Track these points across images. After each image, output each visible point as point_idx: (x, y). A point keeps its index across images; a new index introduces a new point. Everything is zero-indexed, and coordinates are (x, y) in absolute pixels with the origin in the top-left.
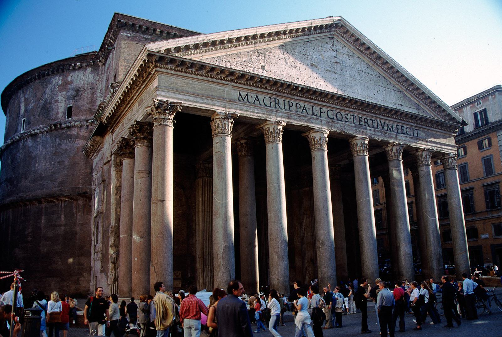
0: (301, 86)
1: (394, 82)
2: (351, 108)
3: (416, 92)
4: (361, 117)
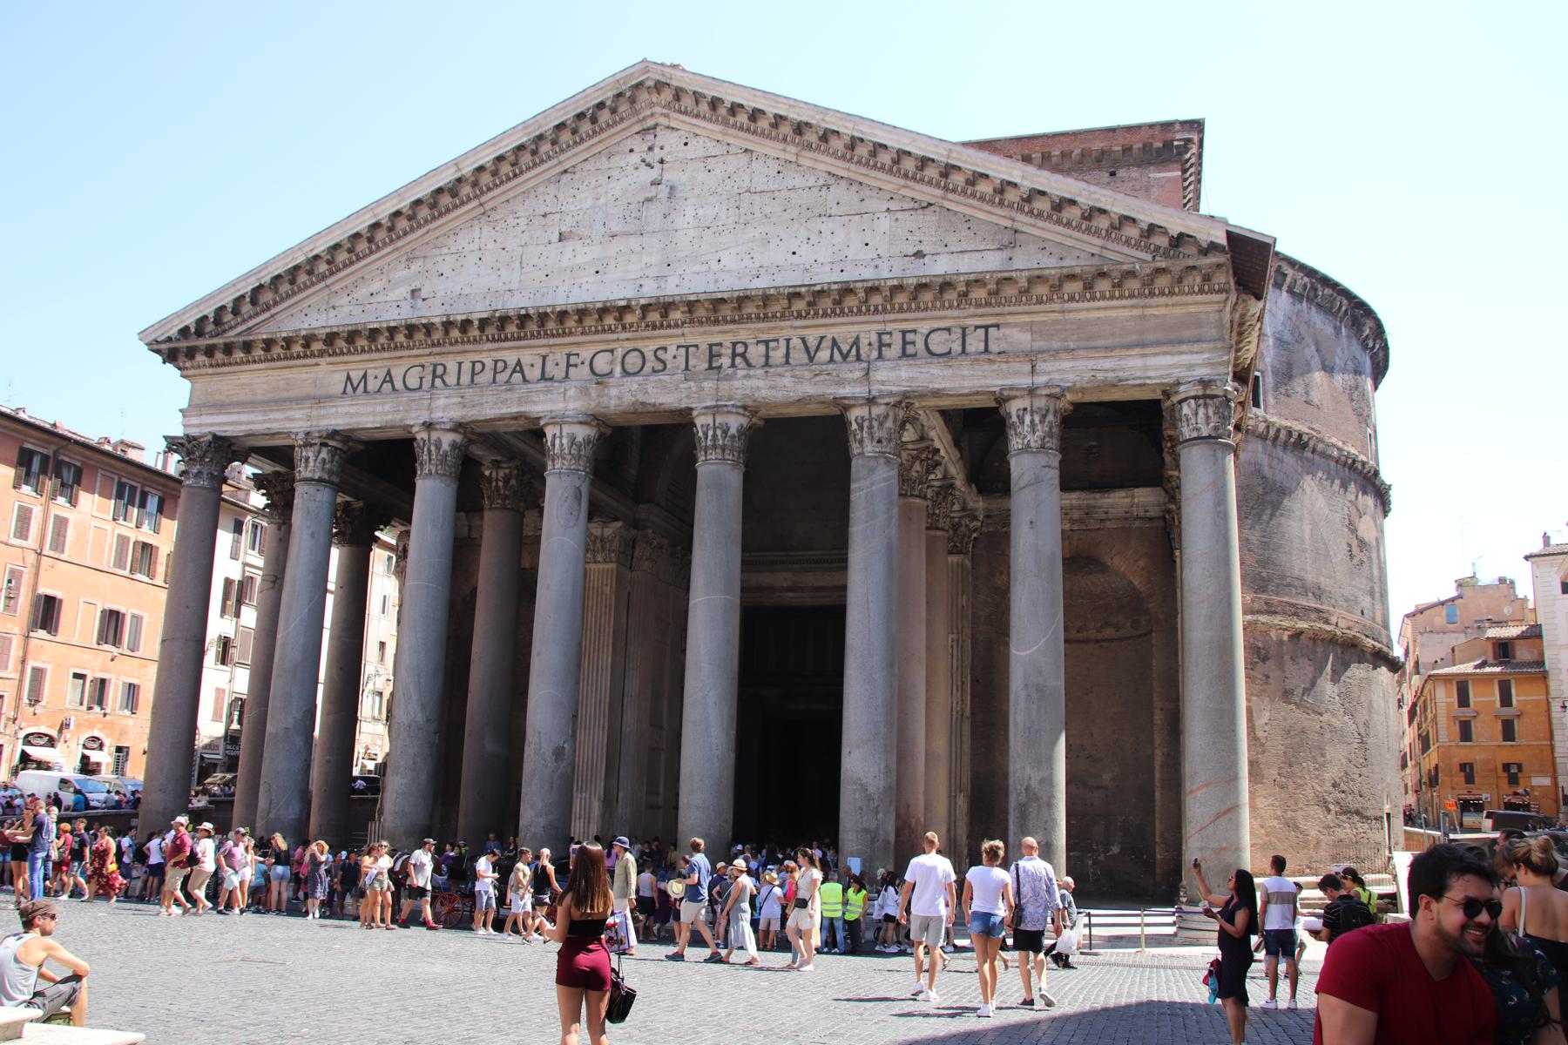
1: (891, 183)
2: (669, 326)
3: (984, 188)
4: (720, 344)
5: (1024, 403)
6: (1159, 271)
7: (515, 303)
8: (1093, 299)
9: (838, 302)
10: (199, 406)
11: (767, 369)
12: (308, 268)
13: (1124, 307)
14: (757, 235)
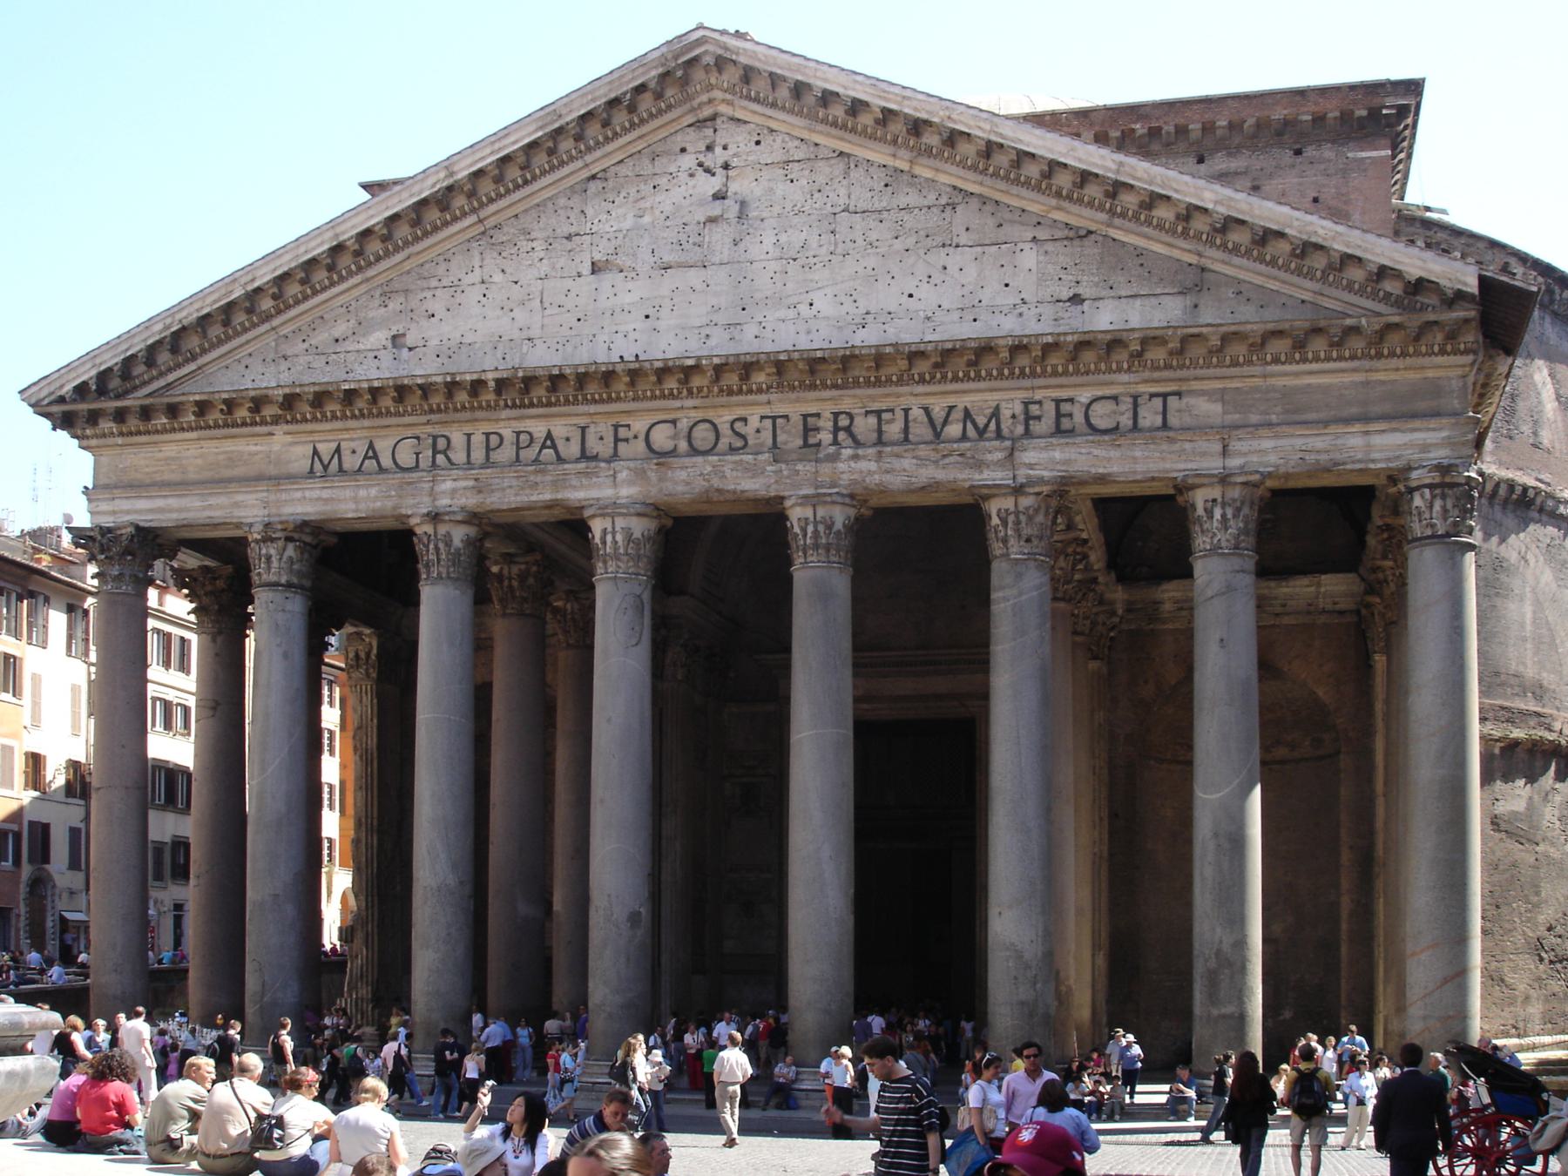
0: (490, 376)
2: (750, 391)
3: (1163, 213)
4: (818, 415)
6: (1390, 327)
7: (542, 358)
8: (1304, 360)
9: (972, 364)
11: (879, 448)
12: (248, 305)
13: (1343, 371)
14: (860, 270)
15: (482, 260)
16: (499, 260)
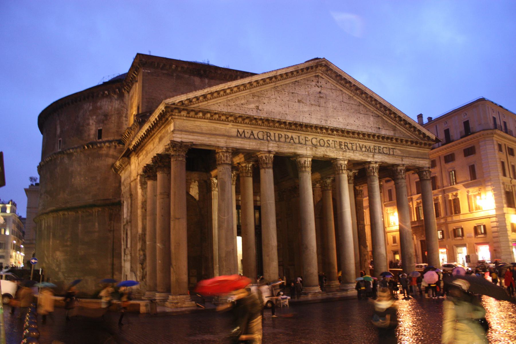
0: (288, 121)
1: (372, 109)
2: (333, 135)
4: (342, 142)
5: (402, 168)
8: (412, 146)
10: (178, 130)
15: (275, 93)
16: (278, 94)
